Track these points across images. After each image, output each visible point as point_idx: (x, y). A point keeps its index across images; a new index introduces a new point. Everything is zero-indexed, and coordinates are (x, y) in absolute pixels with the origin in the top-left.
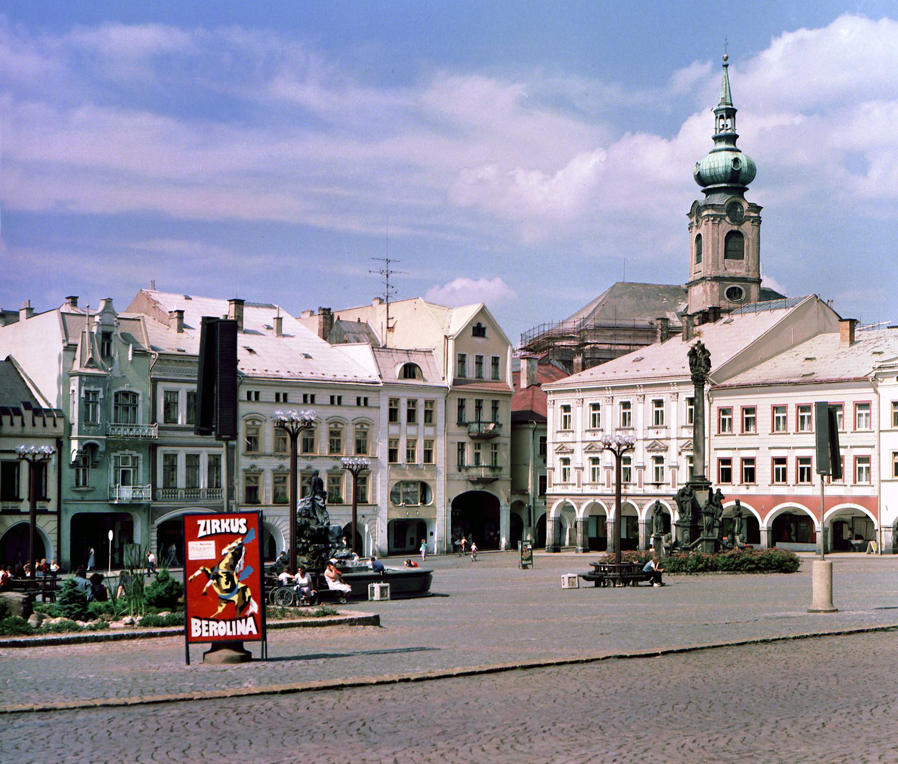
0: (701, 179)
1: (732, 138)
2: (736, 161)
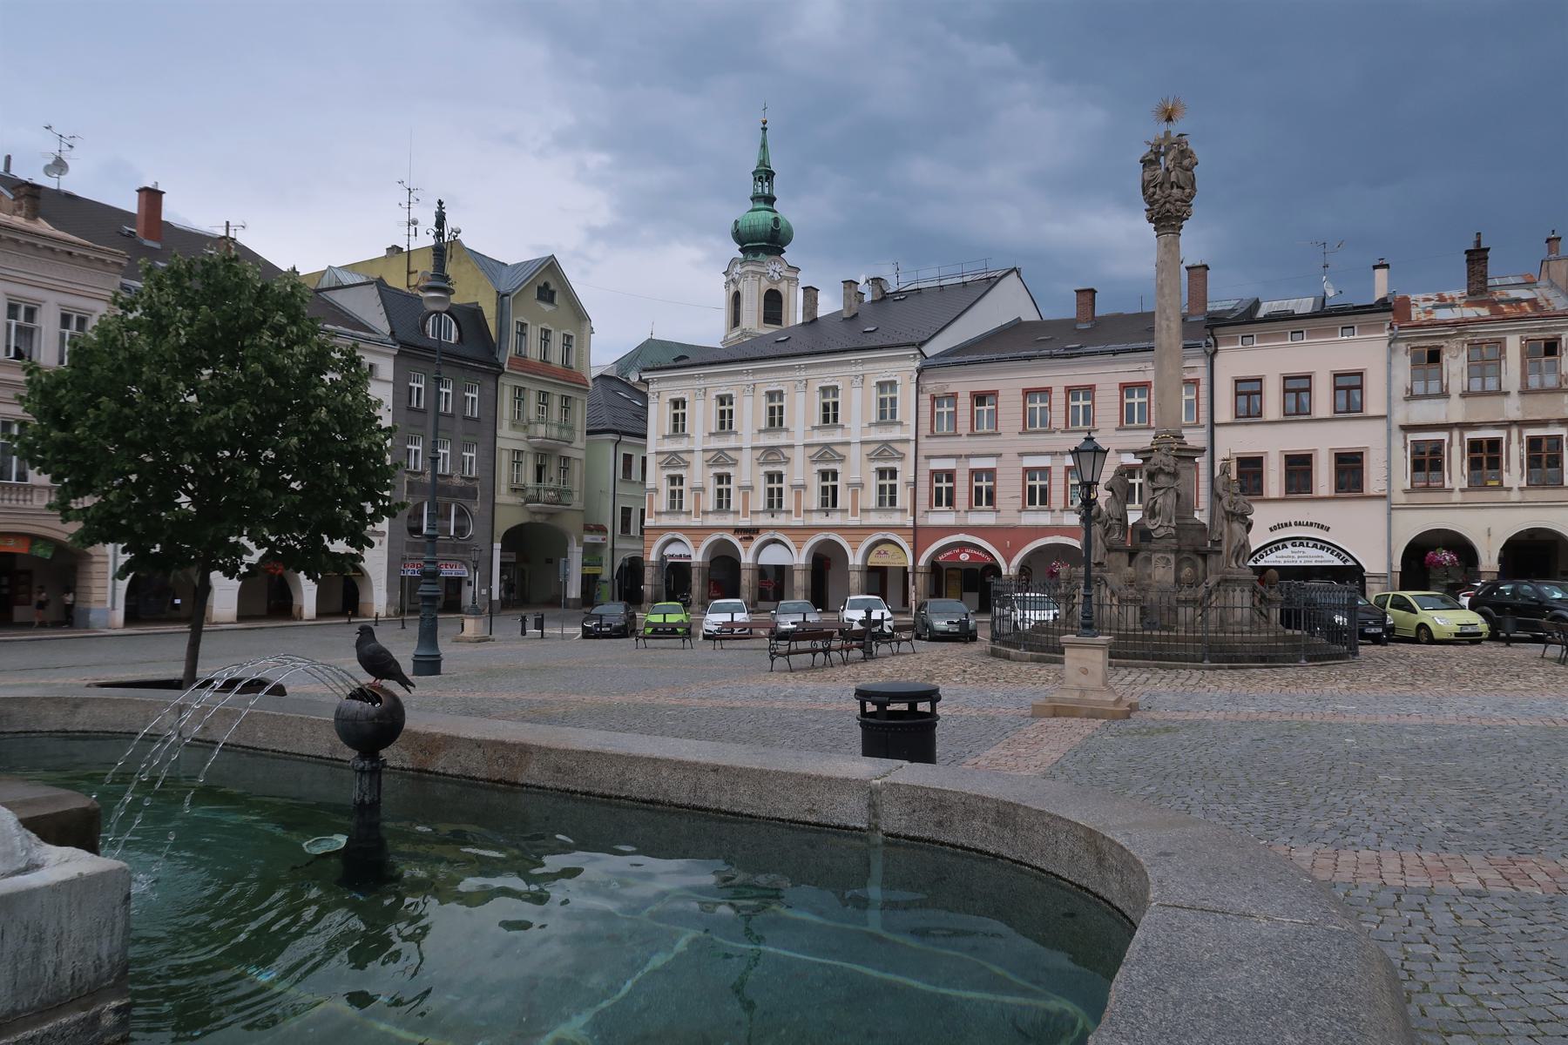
0: (739, 236)
1: (770, 200)
2: (776, 220)
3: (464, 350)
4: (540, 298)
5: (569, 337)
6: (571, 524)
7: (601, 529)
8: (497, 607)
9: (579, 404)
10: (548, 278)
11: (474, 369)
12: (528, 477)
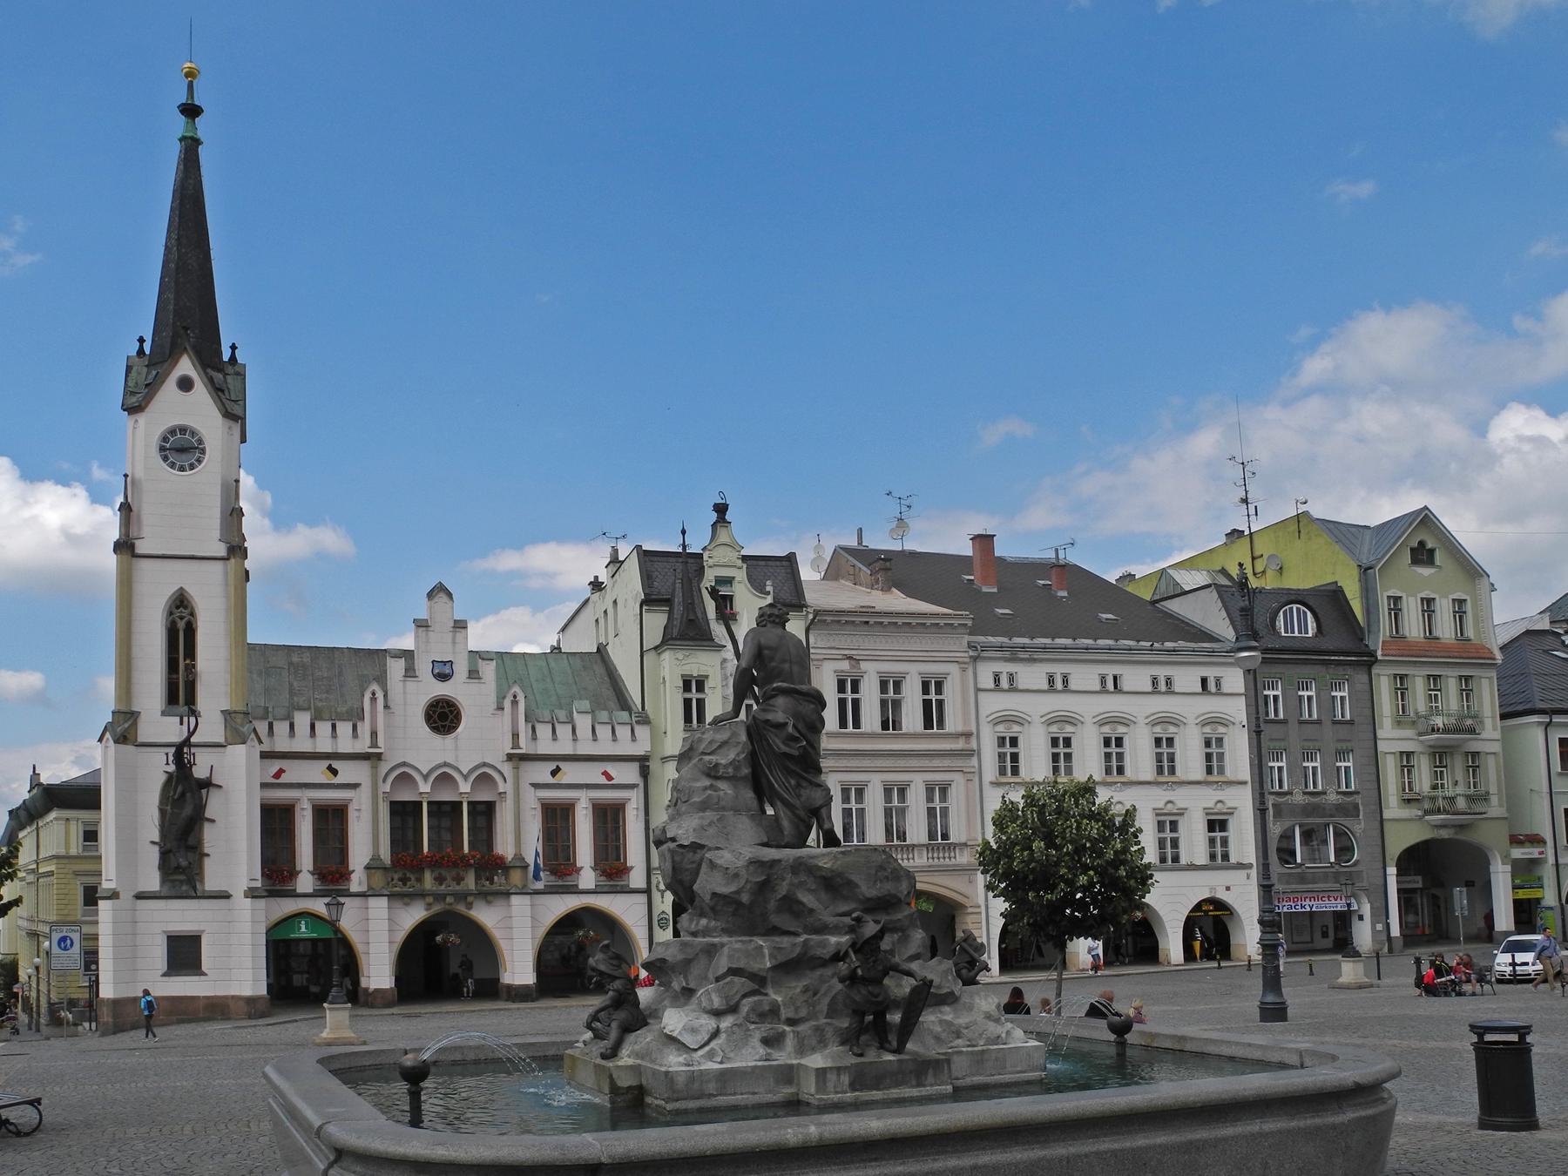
3: (1327, 644)
4: (1416, 561)
5: (1461, 602)
6: (1490, 836)
7: (1536, 840)
8: (1398, 945)
9: (1485, 682)
10: (1423, 535)
11: (1339, 663)
12: (1423, 780)
